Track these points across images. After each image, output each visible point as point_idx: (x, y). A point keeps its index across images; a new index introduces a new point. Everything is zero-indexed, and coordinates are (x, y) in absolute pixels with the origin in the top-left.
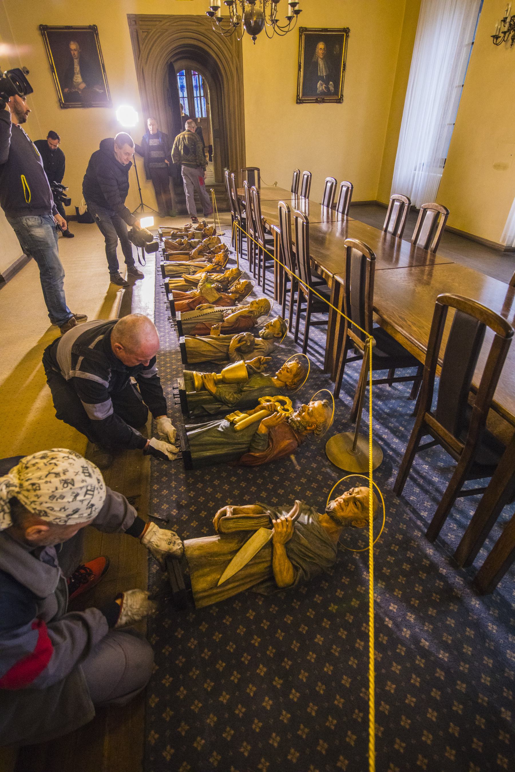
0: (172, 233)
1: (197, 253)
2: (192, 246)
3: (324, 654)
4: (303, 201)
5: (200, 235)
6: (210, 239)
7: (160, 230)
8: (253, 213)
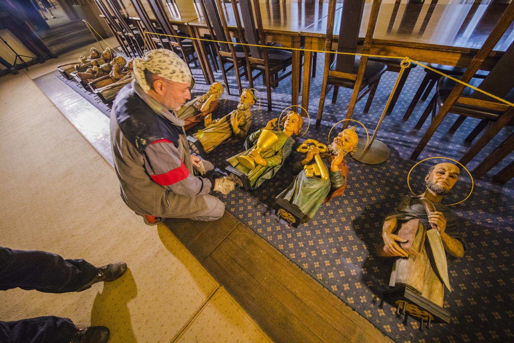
0: (75, 66)
1: (117, 74)
2: (106, 71)
3: (502, 274)
4: (171, 6)
5: (102, 61)
6: (115, 60)
7: (59, 69)
8: (144, 27)
